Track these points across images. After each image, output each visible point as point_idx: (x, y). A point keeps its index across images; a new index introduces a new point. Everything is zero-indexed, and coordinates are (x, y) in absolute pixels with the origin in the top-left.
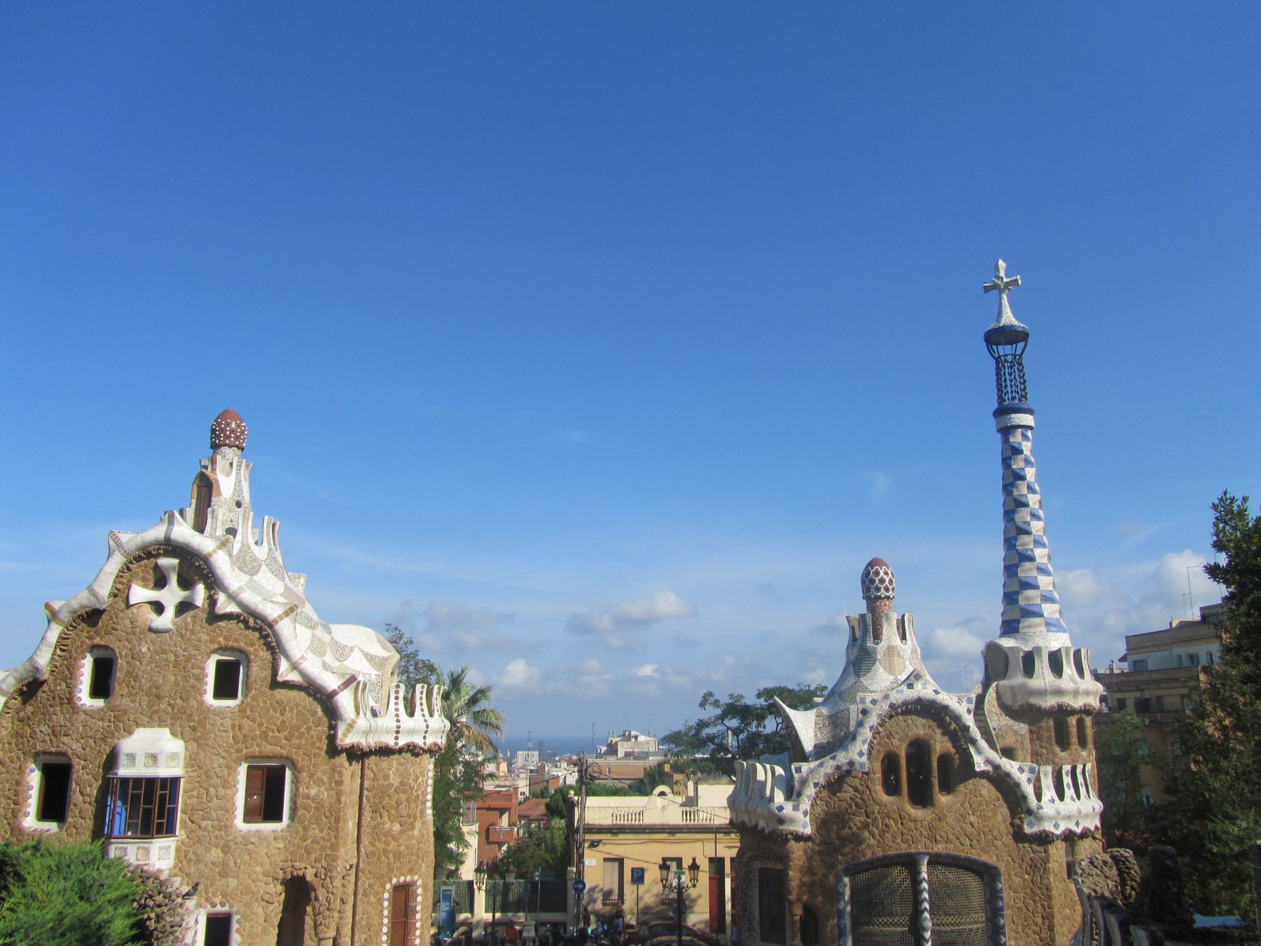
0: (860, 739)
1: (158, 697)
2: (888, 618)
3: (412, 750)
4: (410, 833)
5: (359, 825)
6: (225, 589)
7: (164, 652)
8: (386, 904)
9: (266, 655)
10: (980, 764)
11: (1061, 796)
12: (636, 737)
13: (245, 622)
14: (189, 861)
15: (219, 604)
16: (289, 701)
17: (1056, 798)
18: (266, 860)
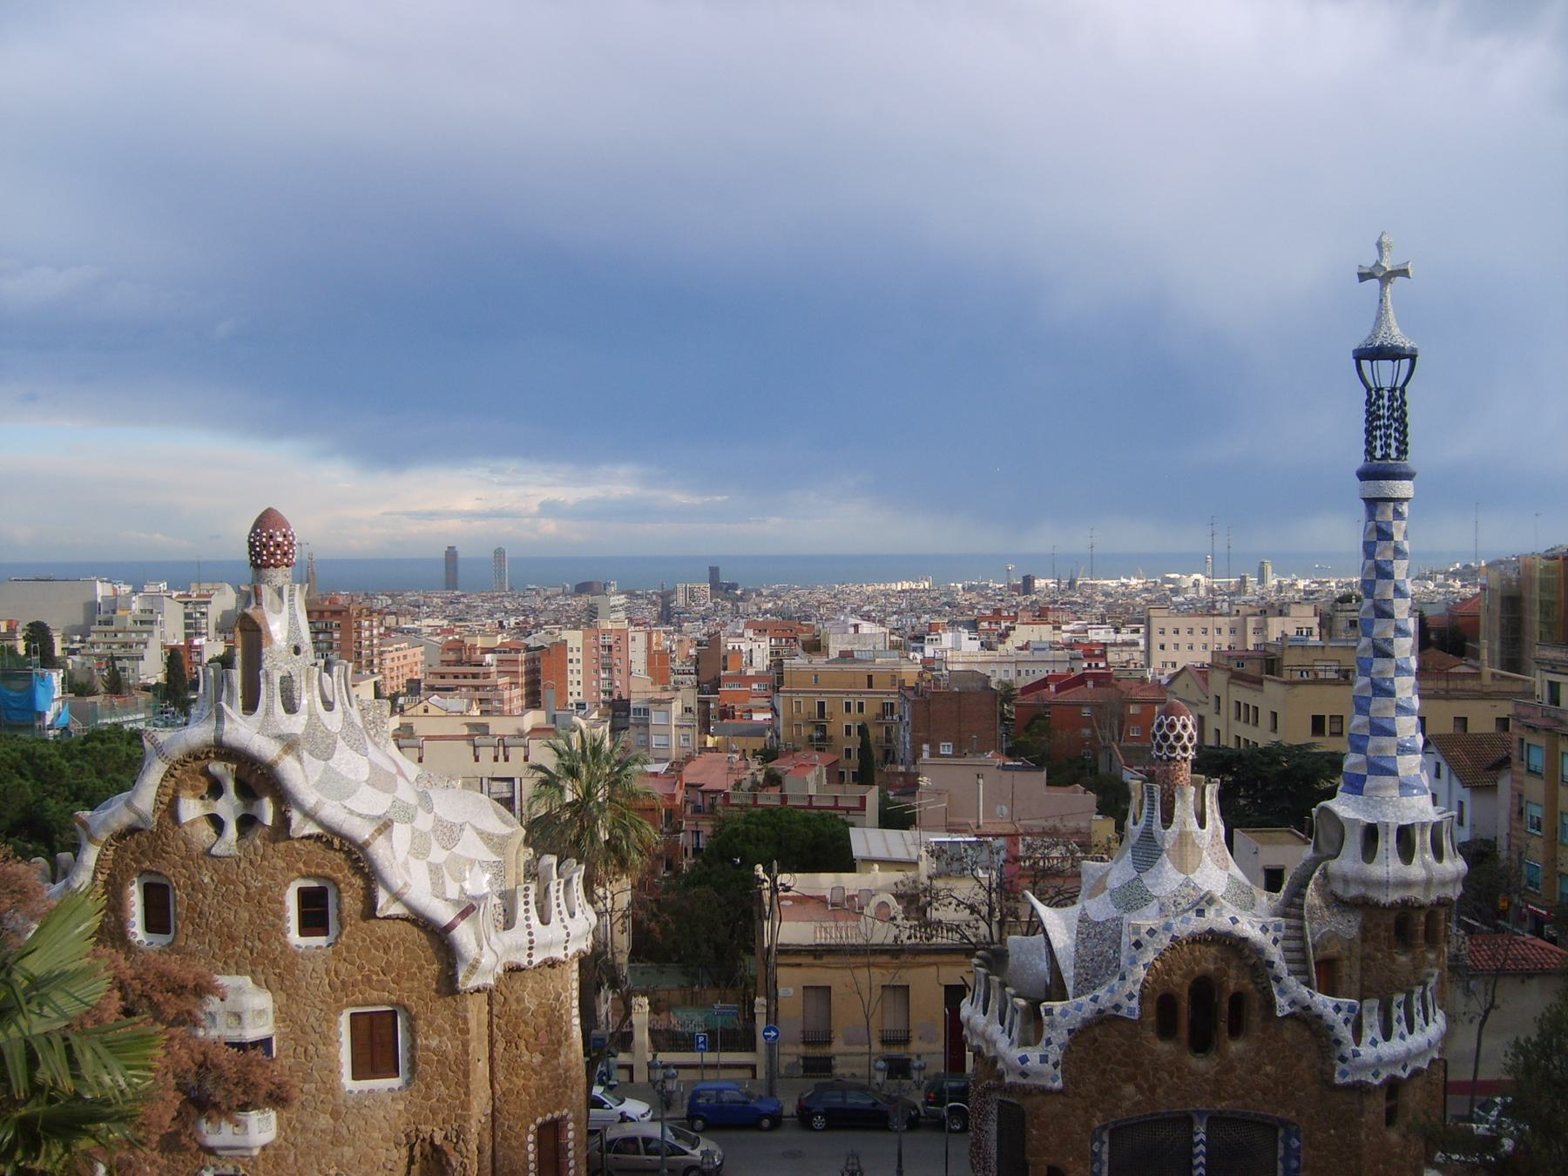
0: (1130, 979)
1: (232, 938)
2: (1183, 795)
3: (552, 964)
4: (555, 1062)
5: (491, 1058)
6: (300, 807)
7: (232, 882)
8: (531, 1147)
9: (358, 882)
10: (1283, 1006)
11: (1387, 1036)
12: (856, 626)
13: (329, 844)
14: (294, 1129)
15: (294, 824)
16: (393, 936)
17: (1380, 1038)
18: (385, 1125)
